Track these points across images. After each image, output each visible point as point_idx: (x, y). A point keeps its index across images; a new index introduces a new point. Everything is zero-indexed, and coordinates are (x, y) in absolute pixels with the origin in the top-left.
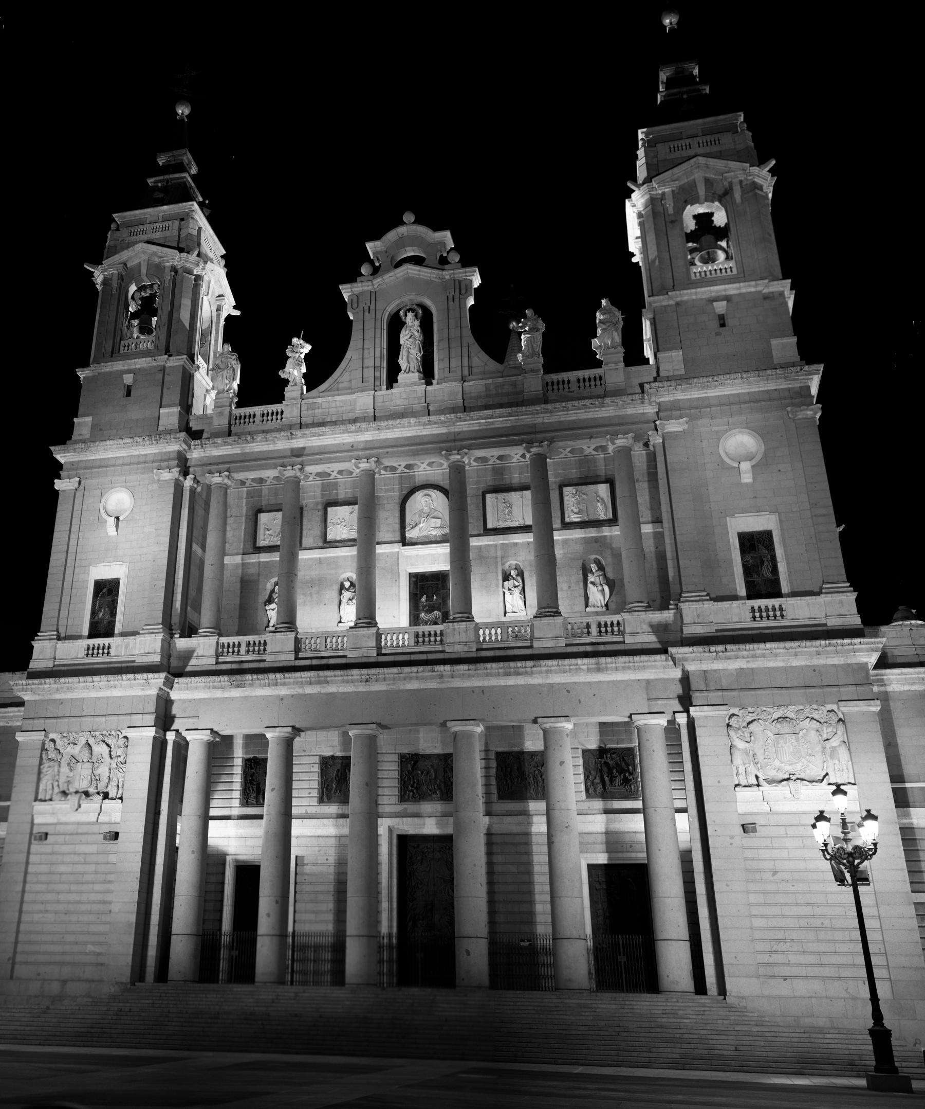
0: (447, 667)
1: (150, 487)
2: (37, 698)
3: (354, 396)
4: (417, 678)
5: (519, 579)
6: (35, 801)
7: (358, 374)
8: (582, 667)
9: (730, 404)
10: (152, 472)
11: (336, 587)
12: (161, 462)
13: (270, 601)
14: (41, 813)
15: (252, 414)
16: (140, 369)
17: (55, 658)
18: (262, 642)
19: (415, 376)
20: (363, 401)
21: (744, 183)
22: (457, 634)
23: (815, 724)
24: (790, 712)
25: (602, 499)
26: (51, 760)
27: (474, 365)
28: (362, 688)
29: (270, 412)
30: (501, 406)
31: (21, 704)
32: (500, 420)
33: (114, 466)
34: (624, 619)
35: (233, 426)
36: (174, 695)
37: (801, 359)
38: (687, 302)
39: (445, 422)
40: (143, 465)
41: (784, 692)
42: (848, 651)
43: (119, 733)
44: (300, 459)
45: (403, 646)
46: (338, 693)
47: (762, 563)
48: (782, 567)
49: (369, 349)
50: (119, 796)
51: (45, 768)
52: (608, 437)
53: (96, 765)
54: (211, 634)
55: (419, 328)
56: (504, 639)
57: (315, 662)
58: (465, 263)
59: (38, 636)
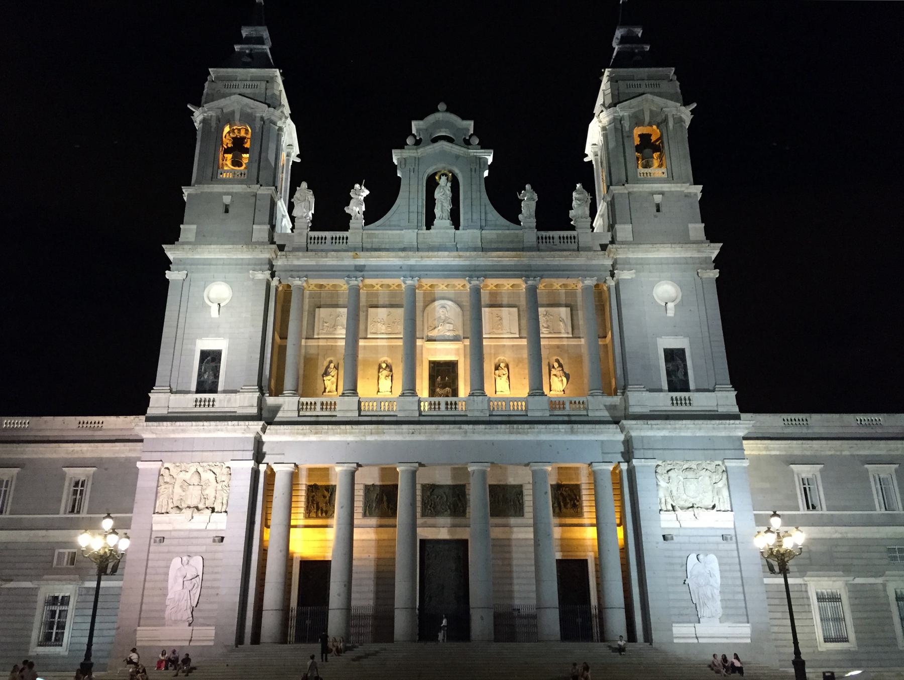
0: (471, 426)
1: (245, 283)
2: (154, 436)
3: (403, 232)
4: (449, 433)
5: (506, 369)
6: (154, 513)
7: (406, 216)
8: (562, 430)
9: (661, 264)
10: (248, 272)
11: (377, 367)
12: (256, 265)
13: (326, 373)
14: (158, 523)
15: (324, 237)
16: (236, 193)
17: (168, 407)
18: (333, 403)
19: (448, 222)
20: (409, 236)
21: (675, 117)
22: (476, 404)
23: (708, 473)
24: (693, 465)
25: (563, 320)
26: (166, 483)
27: (489, 219)
28: (408, 438)
29: (338, 236)
30: (508, 250)
31: (141, 441)
32: (507, 259)
33: (216, 265)
34: (587, 401)
35: (309, 244)
36: (265, 438)
37: (707, 239)
38: (636, 192)
39: (469, 257)
40: (240, 266)
41: (691, 452)
42: (732, 428)
43: (222, 464)
44: (362, 273)
45: (373, 410)
46: (390, 441)
47: (678, 369)
49: (414, 198)
50: (223, 510)
51: (162, 489)
52: (580, 278)
53: (204, 487)
54: (294, 395)
55: (450, 189)
56: (507, 409)
57: (374, 419)
58: (483, 146)
59: (153, 389)
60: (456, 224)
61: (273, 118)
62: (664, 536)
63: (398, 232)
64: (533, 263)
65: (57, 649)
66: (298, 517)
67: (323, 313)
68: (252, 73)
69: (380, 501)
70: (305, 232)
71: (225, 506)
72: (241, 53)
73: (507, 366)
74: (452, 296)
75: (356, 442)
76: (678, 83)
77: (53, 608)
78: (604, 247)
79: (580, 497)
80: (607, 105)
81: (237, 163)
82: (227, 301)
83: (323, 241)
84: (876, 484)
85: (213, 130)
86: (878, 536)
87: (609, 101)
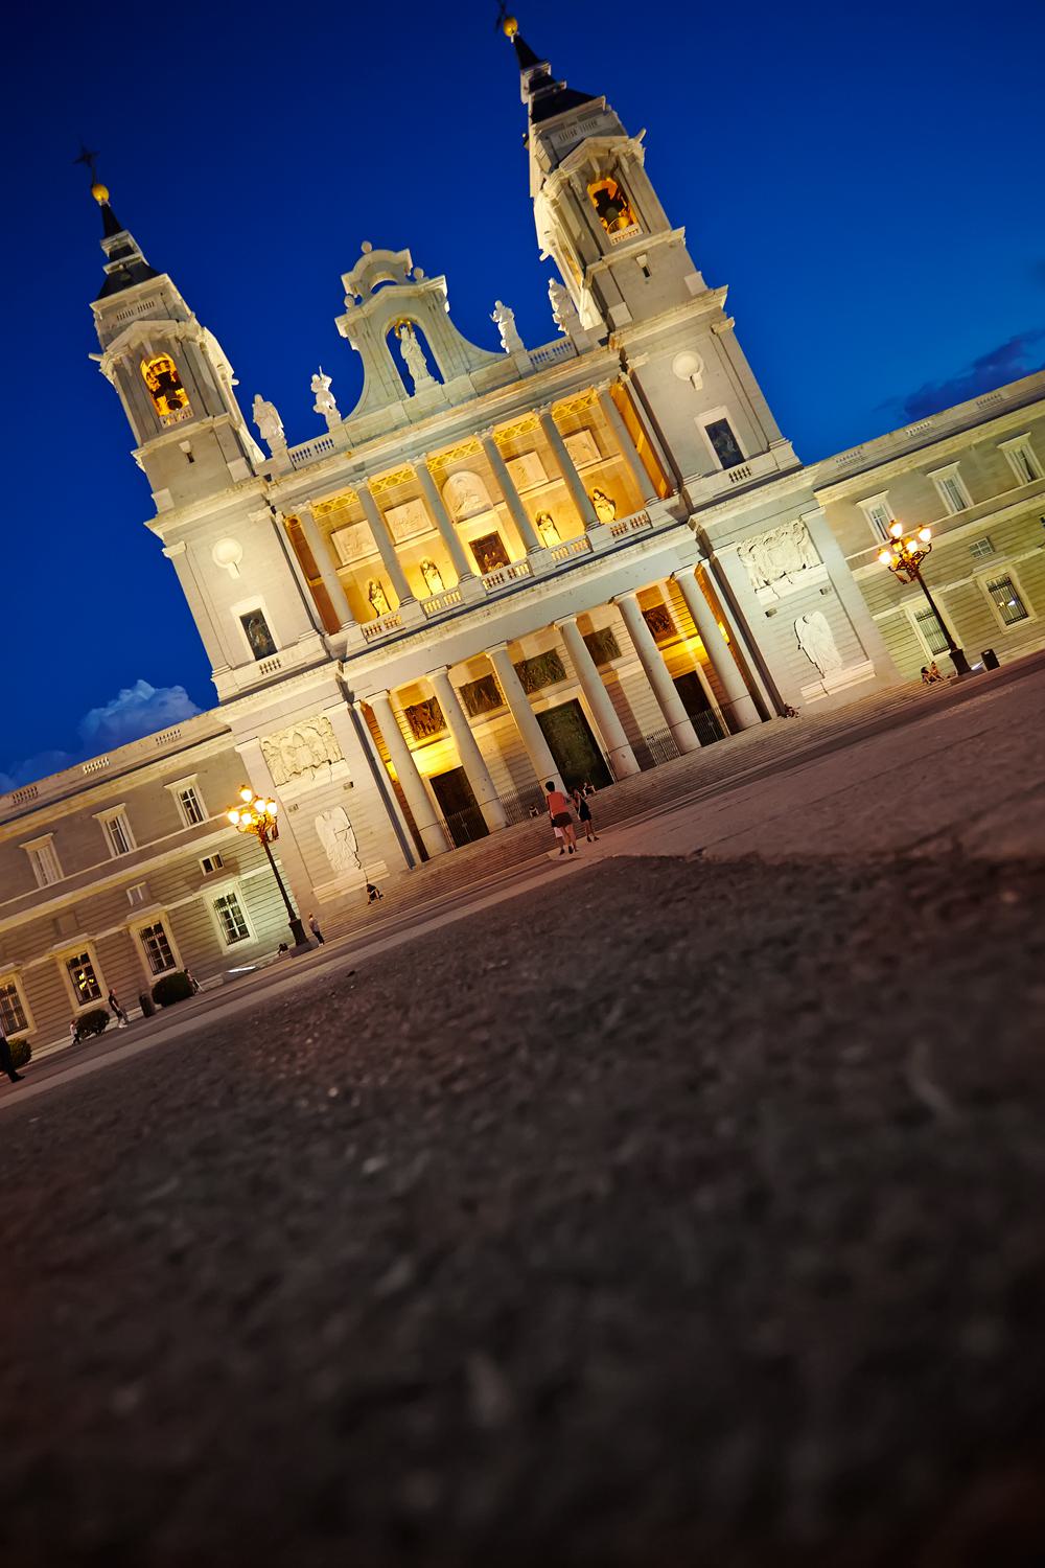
0: (543, 584)
2: (238, 717)
9: (672, 334)
12: (251, 505)
13: (372, 597)
19: (430, 379)
24: (772, 533)
32: (509, 395)
36: (345, 678)
37: (709, 287)
38: (616, 263)
48: (739, 441)
57: (444, 616)
60: (439, 378)
61: (189, 334)
62: (767, 613)
63: (381, 412)
64: (537, 389)
65: (247, 940)
66: (412, 743)
67: (339, 537)
68: (140, 291)
69: (479, 696)
70: (285, 453)
71: (339, 755)
72: (116, 274)
73: (549, 517)
74: (464, 466)
75: (436, 645)
76: (615, 113)
77: (224, 909)
78: (604, 342)
79: (668, 615)
80: (547, 169)
81: (174, 404)
82: (240, 557)
83: (308, 454)
84: (942, 489)
85: (131, 374)
86: (957, 539)
87: (548, 164)
